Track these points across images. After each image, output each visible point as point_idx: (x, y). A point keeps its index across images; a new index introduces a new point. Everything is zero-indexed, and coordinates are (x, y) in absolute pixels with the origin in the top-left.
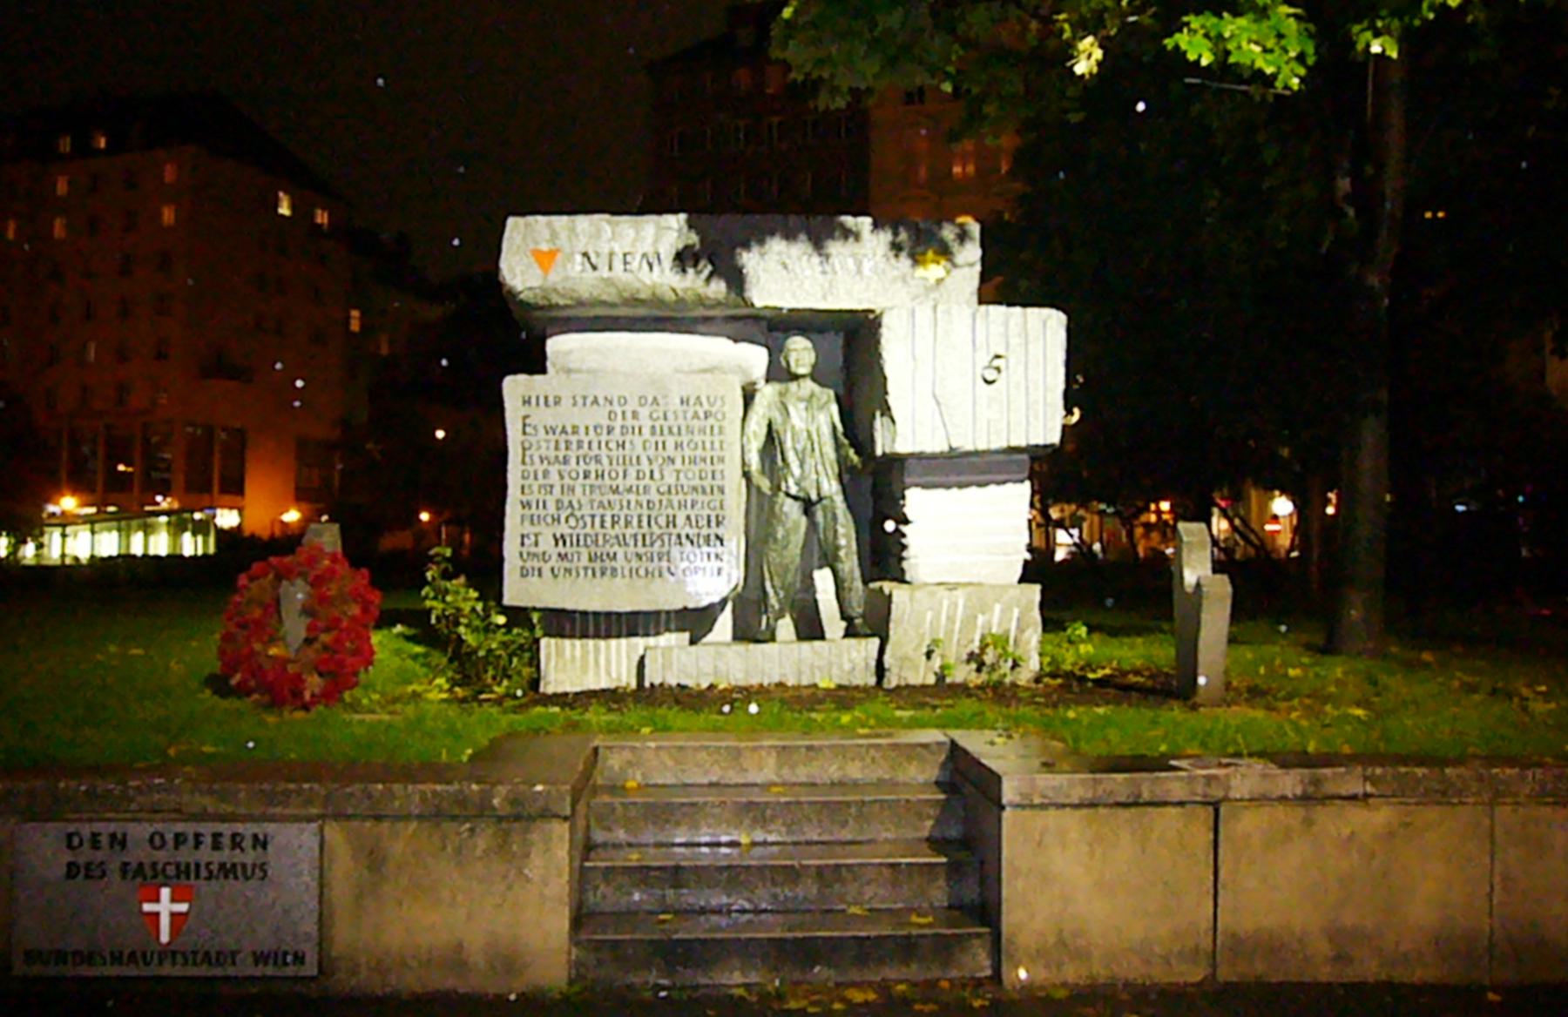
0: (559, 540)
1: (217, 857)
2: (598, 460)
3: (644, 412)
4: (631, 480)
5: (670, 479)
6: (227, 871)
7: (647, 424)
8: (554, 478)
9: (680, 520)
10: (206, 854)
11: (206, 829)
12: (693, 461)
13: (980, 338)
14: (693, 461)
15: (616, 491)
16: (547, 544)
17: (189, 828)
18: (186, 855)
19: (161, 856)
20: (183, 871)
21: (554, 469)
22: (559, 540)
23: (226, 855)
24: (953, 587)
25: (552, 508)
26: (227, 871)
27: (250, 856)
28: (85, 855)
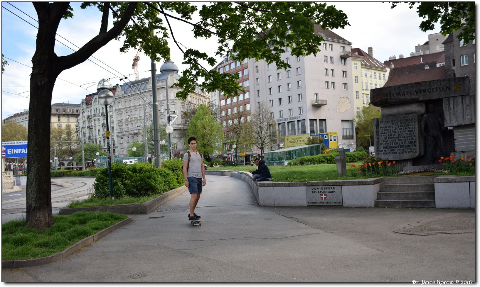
0: (384, 148)
1: (329, 191)
2: (391, 132)
3: (399, 123)
4: (397, 136)
5: (405, 135)
6: (331, 192)
7: (400, 125)
8: (383, 137)
9: (407, 142)
10: (328, 190)
11: (328, 187)
12: (409, 131)
13: (464, 102)
14: (409, 131)
15: (394, 138)
16: (382, 149)
17: (326, 187)
18: (326, 190)
19: (323, 190)
20: (325, 192)
21: (382, 135)
22: (384, 148)
23: (330, 190)
24: (463, 152)
25: (382, 142)
26: (331, 192)
27: (333, 190)
28: (314, 190)
